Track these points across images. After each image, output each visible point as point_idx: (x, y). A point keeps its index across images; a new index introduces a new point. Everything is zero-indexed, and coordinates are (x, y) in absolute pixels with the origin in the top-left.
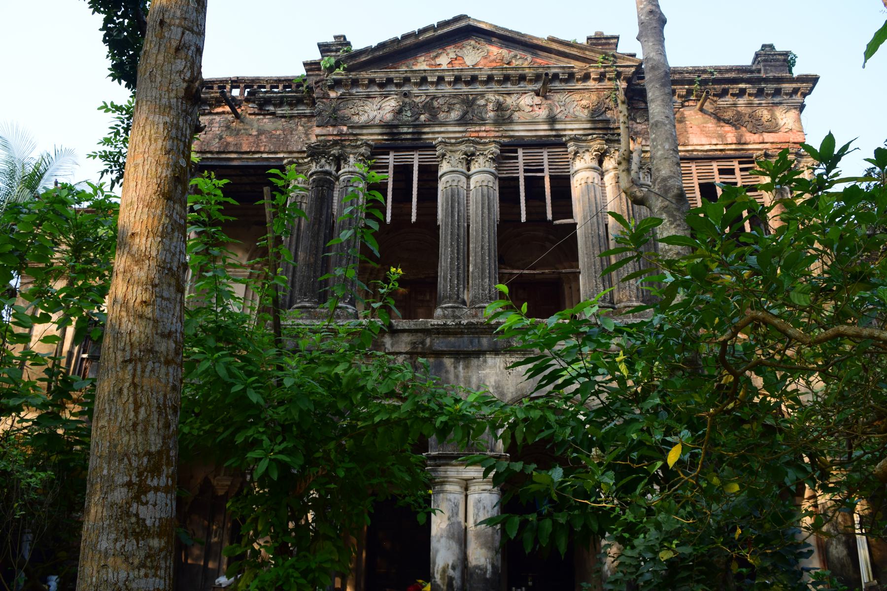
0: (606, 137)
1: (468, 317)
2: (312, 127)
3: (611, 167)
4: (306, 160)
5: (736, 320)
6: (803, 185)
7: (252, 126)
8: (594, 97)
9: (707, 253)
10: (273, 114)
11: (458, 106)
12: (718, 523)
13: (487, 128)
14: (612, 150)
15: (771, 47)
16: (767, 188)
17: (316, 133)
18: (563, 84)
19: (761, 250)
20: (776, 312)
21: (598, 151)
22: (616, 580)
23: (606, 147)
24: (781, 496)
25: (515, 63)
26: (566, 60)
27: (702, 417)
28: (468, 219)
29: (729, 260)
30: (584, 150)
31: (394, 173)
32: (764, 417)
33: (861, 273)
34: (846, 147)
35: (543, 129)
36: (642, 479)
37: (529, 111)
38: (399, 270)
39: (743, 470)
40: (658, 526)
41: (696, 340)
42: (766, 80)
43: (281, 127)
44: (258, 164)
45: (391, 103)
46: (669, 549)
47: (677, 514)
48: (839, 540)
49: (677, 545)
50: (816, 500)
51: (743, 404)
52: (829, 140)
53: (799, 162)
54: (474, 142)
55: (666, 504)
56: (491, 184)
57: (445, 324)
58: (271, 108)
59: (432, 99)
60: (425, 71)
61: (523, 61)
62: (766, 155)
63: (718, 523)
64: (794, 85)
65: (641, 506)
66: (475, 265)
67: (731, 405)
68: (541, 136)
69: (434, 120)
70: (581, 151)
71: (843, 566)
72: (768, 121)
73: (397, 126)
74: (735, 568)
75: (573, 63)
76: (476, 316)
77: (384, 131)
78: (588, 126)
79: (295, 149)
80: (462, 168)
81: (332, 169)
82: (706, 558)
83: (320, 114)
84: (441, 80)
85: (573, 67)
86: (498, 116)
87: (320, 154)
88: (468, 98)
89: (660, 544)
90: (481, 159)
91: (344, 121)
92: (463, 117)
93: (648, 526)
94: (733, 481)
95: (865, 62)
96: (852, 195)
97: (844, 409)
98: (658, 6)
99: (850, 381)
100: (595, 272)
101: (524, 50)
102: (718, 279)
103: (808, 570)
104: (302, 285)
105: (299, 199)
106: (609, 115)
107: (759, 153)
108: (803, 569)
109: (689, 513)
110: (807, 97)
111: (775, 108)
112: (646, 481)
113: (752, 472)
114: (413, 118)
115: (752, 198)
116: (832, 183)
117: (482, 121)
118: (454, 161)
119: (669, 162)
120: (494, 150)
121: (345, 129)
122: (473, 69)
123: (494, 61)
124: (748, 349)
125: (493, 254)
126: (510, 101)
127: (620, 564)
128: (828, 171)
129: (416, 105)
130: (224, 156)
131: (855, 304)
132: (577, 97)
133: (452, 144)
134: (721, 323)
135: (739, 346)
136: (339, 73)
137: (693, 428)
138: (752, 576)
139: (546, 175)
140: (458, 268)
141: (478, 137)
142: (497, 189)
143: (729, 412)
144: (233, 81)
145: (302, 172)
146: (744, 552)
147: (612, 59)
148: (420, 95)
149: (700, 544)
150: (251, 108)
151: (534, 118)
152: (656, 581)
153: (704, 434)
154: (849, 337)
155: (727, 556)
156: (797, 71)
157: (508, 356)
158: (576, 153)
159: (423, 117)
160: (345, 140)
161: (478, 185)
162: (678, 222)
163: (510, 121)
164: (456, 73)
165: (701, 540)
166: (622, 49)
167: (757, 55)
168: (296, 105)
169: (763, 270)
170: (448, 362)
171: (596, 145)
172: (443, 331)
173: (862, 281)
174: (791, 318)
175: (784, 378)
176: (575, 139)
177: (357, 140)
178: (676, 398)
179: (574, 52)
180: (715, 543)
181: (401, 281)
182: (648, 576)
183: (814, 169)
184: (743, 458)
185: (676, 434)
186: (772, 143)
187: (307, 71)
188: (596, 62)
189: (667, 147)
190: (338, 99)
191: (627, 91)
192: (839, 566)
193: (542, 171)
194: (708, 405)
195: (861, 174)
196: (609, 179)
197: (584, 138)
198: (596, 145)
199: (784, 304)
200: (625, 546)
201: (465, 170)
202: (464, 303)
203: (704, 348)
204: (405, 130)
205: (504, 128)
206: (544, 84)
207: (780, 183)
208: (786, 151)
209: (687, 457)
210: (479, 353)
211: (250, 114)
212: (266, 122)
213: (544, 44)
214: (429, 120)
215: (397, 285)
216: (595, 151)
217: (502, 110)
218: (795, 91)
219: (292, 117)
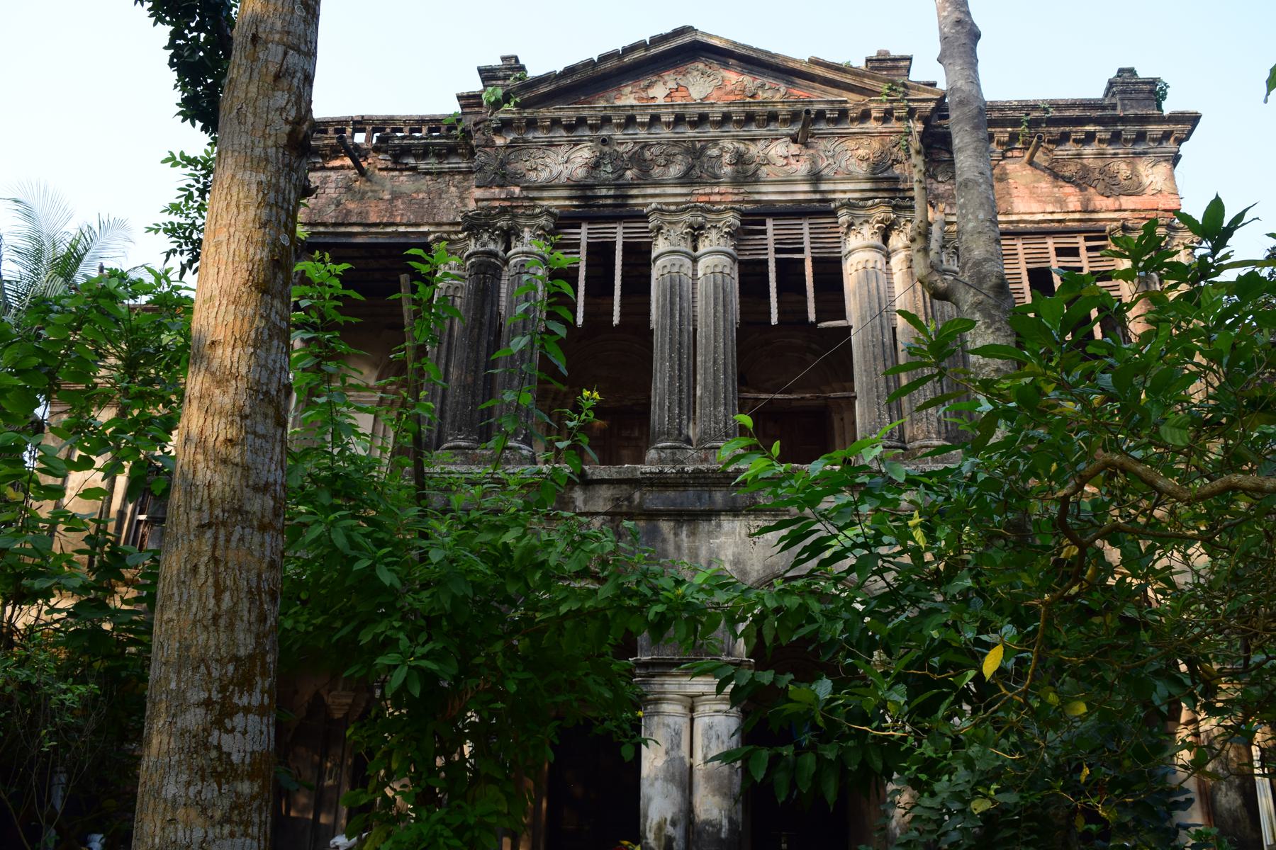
0: (894, 202)
1: (695, 462)
2: (469, 188)
3: (900, 245)
4: (461, 236)
5: (1082, 466)
6: (1178, 271)
7: (383, 186)
8: (876, 145)
9: (1040, 370)
10: (414, 169)
11: (680, 157)
12: (1056, 759)
13: (722, 189)
14: (902, 221)
15: (1132, 71)
16: (1126, 275)
17: (475, 197)
18: (832, 126)
19: (1117, 365)
20: (1138, 454)
21: (881, 222)
22: (909, 842)
23: (893, 216)
24: (1147, 721)
25: (762, 96)
26: (836, 91)
27: (1032, 607)
28: (695, 321)
29: (1071, 379)
30: (861, 220)
31: (588, 254)
32: (1122, 606)
33: (1263, 398)
34: (1240, 217)
35: (802, 192)
36: (948, 695)
37: (782, 164)
38: (596, 395)
39: (1092, 683)
40: (969, 764)
41: (1024, 495)
42: (1125, 120)
43: (425, 188)
44: (392, 241)
45: (584, 154)
46: (985, 796)
47: (996, 746)
48: (1230, 783)
49: (997, 792)
50: (1197, 726)
51: (1092, 587)
52: (1216, 207)
53: (1172, 238)
54: (702, 209)
55: (981, 732)
56: (727, 271)
57: (661, 472)
58: (411, 161)
59: (642, 148)
60: (632, 107)
61: (774, 93)
62: (1125, 228)
63: (1056, 759)
64: (1165, 127)
65: (944, 735)
66: (705, 387)
67: (1075, 589)
68: (799, 201)
69: (645, 178)
70: (857, 222)
71: (1236, 821)
72: (1127, 178)
73: (592, 187)
74: (1081, 824)
76: (705, 460)
77: (574, 193)
78: (868, 186)
79: (445, 220)
80: (686, 247)
81: (498, 248)
82: (1039, 810)
83: (481, 169)
84: (655, 120)
85: (846, 102)
86: (738, 172)
87: (481, 226)
88: (694, 146)
89: (972, 789)
90: (713, 234)
91: (516, 179)
93: (954, 764)
94: (1078, 699)
95: (1268, 94)
96: (1248, 285)
97: (1237, 595)
98: (968, 14)
99: (1246, 555)
100: (878, 397)
101: (776, 78)
102: (1055, 406)
103: (1186, 827)
104: (455, 416)
105: (451, 292)
106: (897, 170)
107: (1115, 224)
108: (1178, 825)
109: (1014, 744)
110: (1184, 144)
111: (1137, 160)
112: (952, 698)
113: (1106, 686)
114: (615, 175)
115: (1104, 290)
116: (1220, 269)
117: (715, 180)
118: (674, 236)
119: (984, 238)
120: (733, 220)
121: (517, 190)
122: (702, 104)
123: (732, 92)
124: (1099, 508)
125: (730, 372)
126: (754, 150)
127: (915, 818)
128: (1215, 251)
129: (619, 156)
130: (342, 229)
131: (1254, 443)
132: (851, 144)
133: (671, 213)
134: (1060, 470)
135: (1086, 504)
136: (509, 111)
137: (1019, 622)
138: (1105, 835)
139: (808, 257)
140: (681, 391)
141: (709, 202)
142: (736, 276)
143: (1071, 599)
144: (355, 122)
145: (455, 253)
146: (1093, 802)
147: (902, 89)
148: (624, 141)
149: (1029, 789)
150: (382, 160)
151: (790, 175)
152: (966, 843)
153: (1035, 630)
154: (1245, 490)
155: (1068, 807)
156: (1168, 107)
157: (752, 517)
158: (850, 225)
159: (629, 174)
160: (517, 207)
161: (709, 271)
162: (998, 325)
163: (755, 179)
164: (677, 110)
165: (1032, 784)
166: (917, 75)
167: (1111, 84)
168: (446, 156)
169: (1121, 392)
170: (666, 526)
171: (879, 213)
172: (658, 482)
173: (1263, 410)
174: (1160, 462)
175: (1151, 550)
176: (849, 205)
177: (534, 207)
178: (996, 578)
179: (848, 79)
180: (1051, 788)
181: (598, 410)
182: (954, 836)
183: (1194, 249)
184: (1092, 665)
185: (995, 631)
186: (1133, 210)
187: (463, 107)
188: (879, 94)
189: (981, 216)
190: (508, 147)
191: (923, 136)
192: (1231, 822)
193: (801, 251)
194: (1042, 589)
195: (1261, 255)
196: (897, 262)
197: (861, 203)
198: (879, 213)
199: (1150, 444)
200: (921, 793)
201: (690, 250)
202: (689, 441)
203: (1036, 507)
204: (604, 192)
205: (747, 189)
206: (804, 126)
207: (1144, 268)
208: (1153, 223)
209: (1011, 664)
210: (711, 514)
211: (381, 169)
212: (404, 181)
213: (804, 69)
214: (639, 178)
215: (592, 415)
216: (878, 222)
217: (744, 163)
218: (1167, 136)
219: (440, 173)
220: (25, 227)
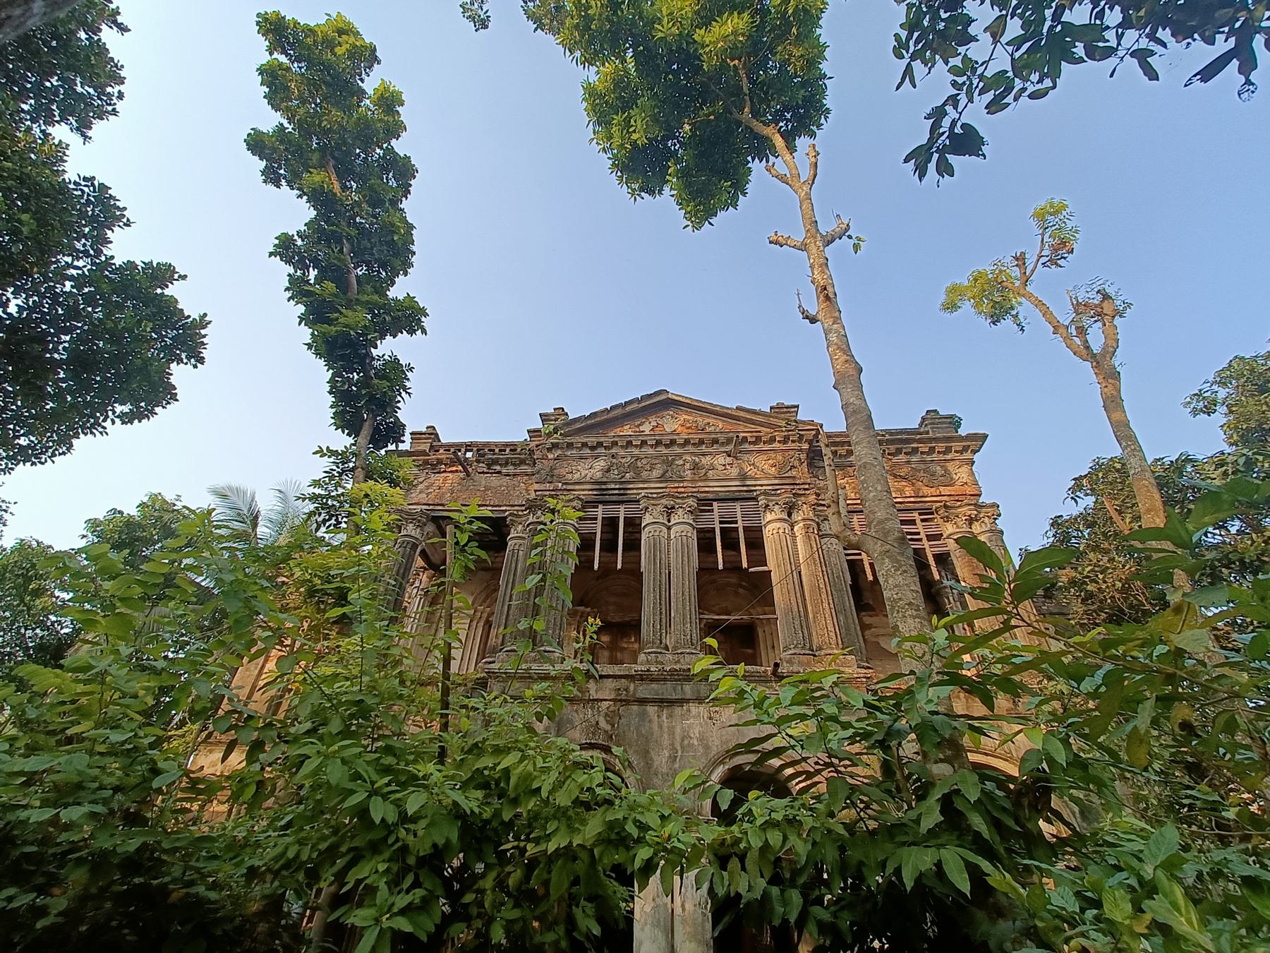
10: (499, 472)
13: (685, 484)
17: (533, 489)
45: (601, 464)
58: (498, 468)
69: (637, 478)
73: (605, 483)
75: (759, 429)
76: (678, 662)
84: (644, 443)
92: (663, 475)
122: (672, 433)
126: (705, 461)
156: (963, 431)
168: (519, 465)
170: (652, 710)
171: (785, 497)
172: (643, 677)
176: (765, 493)
179: (760, 419)
193: (736, 522)
202: (667, 648)
204: (613, 486)
210: (682, 702)
212: (494, 481)
218: (965, 449)
220: (278, 507)
